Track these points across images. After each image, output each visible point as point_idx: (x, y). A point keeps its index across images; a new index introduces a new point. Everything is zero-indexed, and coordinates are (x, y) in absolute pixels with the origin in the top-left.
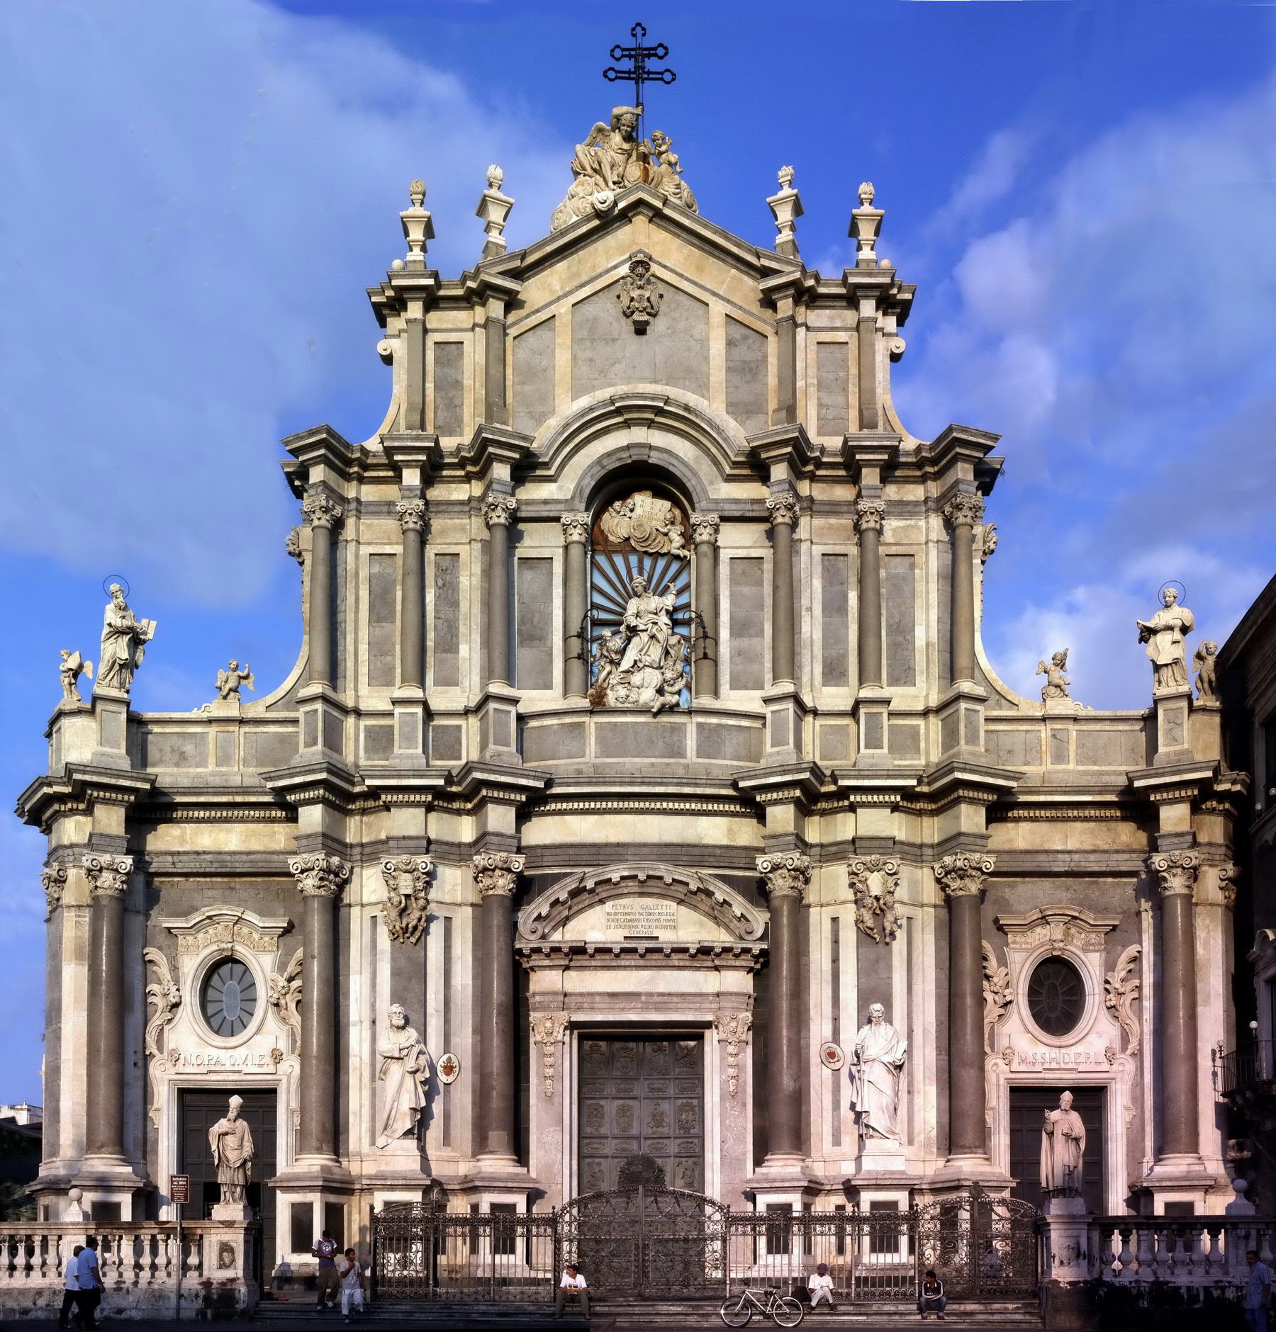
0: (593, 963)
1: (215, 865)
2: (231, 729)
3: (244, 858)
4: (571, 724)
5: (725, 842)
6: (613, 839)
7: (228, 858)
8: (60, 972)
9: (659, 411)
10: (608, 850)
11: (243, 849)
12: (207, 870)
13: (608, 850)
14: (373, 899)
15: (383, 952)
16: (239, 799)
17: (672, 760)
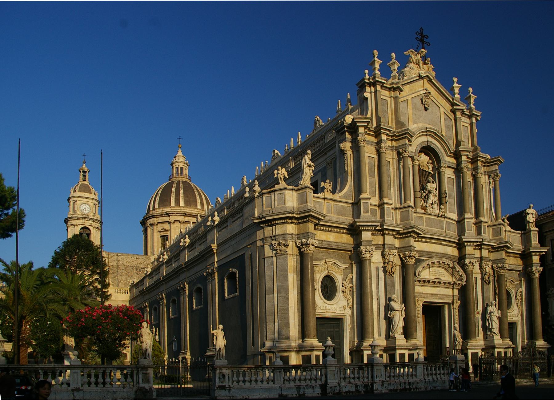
0: (428, 285)
1: (327, 245)
2: (330, 202)
3: (335, 244)
4: (419, 216)
5: (452, 254)
6: (430, 251)
7: (331, 243)
8: (287, 277)
9: (435, 134)
10: (429, 253)
11: (334, 241)
12: (325, 247)
13: (429, 253)
14: (377, 261)
15: (381, 278)
16: (338, 226)
17: (440, 230)
